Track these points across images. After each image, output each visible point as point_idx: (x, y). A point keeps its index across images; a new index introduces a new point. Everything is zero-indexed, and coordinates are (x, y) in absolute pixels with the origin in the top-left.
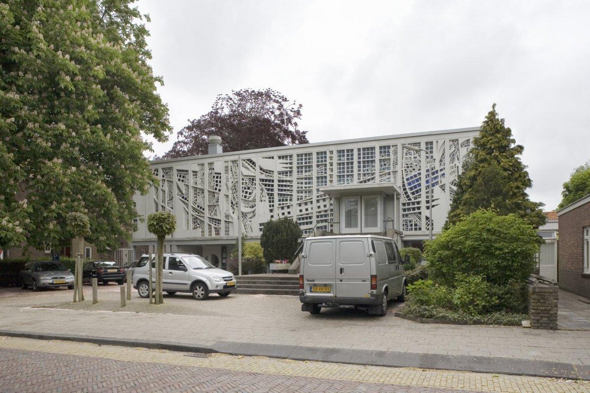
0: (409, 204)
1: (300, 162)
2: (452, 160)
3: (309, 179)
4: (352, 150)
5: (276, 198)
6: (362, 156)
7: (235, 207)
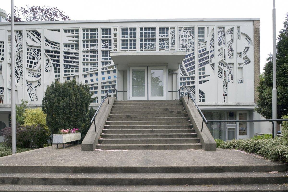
0: (184, 79)
1: (86, 36)
2: (220, 44)
3: (95, 52)
4: (135, 29)
5: (62, 69)
6: (143, 35)
7: (19, 76)
